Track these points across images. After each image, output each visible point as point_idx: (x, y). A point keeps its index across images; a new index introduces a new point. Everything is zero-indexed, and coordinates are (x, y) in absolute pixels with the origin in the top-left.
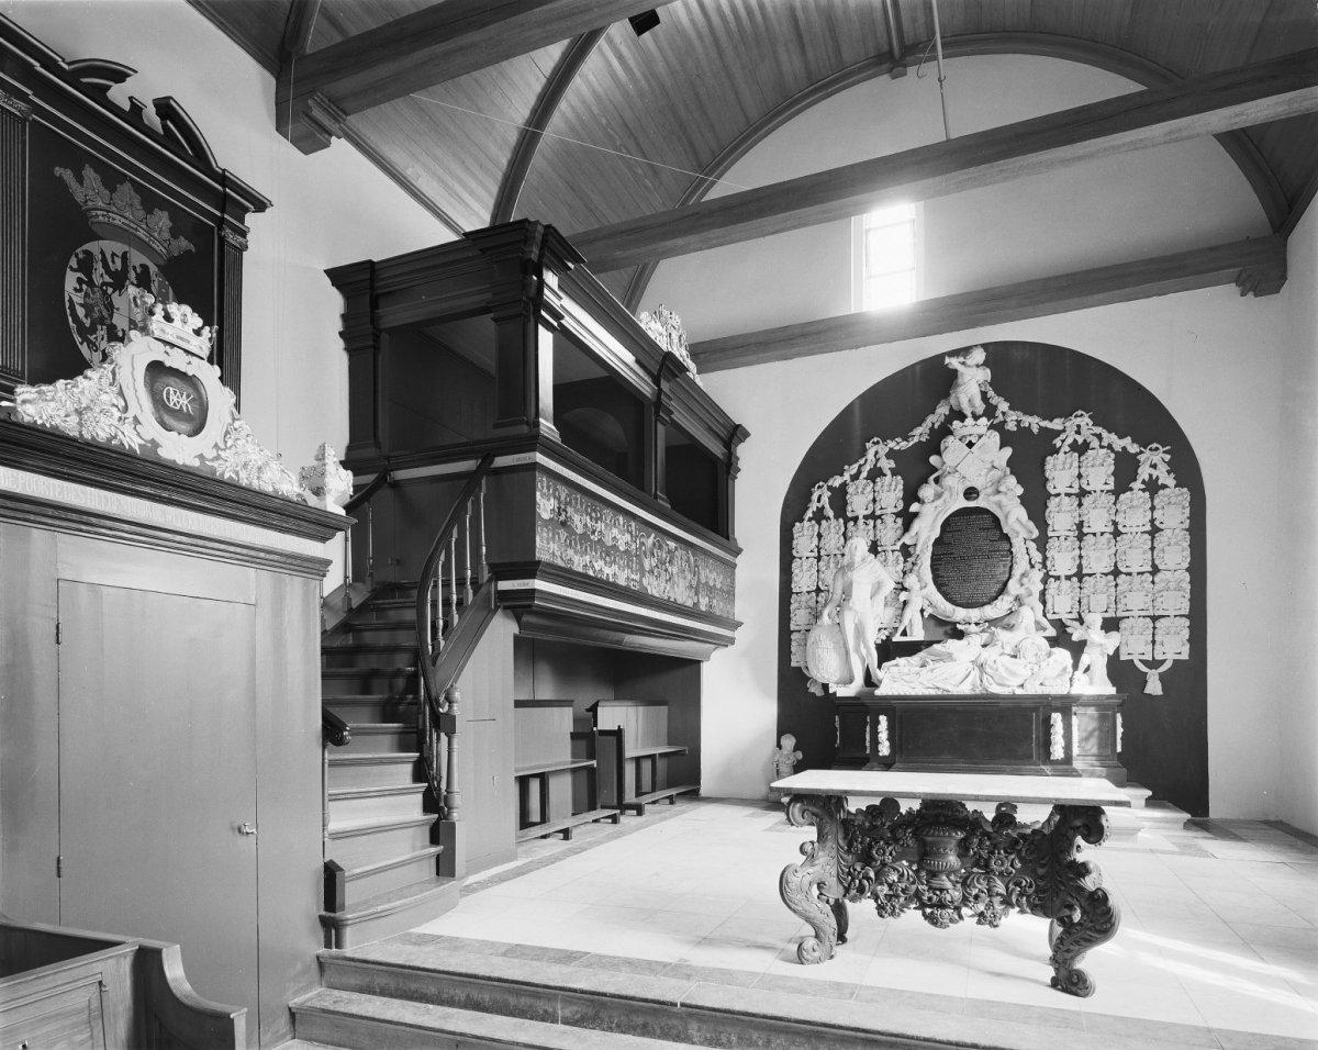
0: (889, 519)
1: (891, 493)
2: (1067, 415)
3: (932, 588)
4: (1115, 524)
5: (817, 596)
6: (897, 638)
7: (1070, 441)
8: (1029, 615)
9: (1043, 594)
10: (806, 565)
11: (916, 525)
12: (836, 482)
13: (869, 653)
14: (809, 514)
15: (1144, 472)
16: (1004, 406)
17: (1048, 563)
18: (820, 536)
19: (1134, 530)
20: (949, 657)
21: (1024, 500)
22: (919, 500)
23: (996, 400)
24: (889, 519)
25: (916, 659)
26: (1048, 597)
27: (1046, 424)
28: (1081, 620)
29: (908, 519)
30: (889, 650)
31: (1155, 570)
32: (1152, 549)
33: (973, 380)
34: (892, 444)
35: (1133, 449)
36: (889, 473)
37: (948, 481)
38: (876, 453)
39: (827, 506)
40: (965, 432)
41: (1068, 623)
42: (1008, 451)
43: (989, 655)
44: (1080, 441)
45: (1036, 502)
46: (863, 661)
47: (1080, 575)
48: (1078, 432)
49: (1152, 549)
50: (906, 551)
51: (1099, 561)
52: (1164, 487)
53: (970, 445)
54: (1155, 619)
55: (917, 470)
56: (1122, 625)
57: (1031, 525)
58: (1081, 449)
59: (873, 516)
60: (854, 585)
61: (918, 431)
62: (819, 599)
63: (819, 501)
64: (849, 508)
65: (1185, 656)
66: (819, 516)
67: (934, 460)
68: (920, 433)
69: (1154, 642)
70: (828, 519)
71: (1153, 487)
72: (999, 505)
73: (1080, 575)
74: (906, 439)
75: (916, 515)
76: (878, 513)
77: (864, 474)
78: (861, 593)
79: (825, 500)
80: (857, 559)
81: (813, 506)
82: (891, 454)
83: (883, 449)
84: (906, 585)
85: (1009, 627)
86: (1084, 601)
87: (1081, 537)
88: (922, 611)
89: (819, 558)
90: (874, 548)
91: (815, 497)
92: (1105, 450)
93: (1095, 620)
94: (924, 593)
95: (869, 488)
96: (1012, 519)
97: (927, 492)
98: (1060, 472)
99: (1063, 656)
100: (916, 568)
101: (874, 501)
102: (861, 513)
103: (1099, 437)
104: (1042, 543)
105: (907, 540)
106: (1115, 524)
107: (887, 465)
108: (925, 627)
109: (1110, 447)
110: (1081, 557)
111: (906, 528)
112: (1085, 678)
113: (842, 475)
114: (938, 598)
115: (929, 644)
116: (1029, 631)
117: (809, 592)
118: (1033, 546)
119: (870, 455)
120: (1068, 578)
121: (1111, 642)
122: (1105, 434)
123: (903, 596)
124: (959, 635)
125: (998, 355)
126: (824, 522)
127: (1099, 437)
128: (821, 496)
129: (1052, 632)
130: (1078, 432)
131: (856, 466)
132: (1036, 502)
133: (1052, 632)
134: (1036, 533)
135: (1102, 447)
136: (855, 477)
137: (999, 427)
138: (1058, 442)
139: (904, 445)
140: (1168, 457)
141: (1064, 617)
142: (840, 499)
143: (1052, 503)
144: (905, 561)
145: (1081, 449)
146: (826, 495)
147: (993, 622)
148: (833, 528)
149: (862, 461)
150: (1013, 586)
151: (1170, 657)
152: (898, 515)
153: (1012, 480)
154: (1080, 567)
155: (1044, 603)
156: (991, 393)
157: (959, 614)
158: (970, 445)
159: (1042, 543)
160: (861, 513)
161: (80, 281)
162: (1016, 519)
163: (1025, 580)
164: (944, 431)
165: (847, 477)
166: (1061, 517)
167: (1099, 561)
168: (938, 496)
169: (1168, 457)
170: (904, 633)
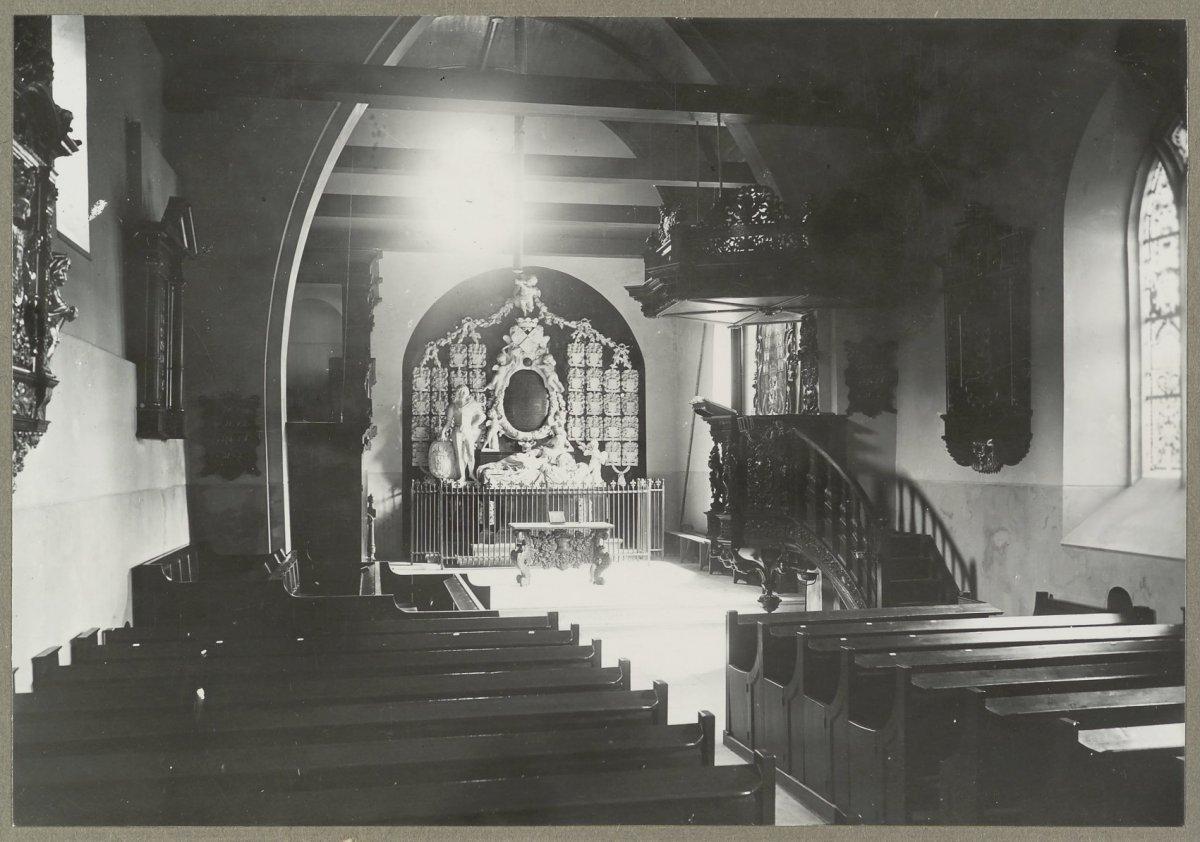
3: (504, 419)
5: (430, 418)
6: (484, 450)
7: (580, 336)
8: (562, 439)
9: (566, 425)
11: (497, 379)
12: (443, 344)
15: (617, 359)
16: (544, 309)
17: (569, 408)
19: (613, 391)
20: (520, 465)
26: (569, 427)
27: (567, 323)
29: (490, 376)
31: (622, 416)
34: (478, 323)
35: (612, 345)
37: (516, 353)
39: (436, 358)
40: (522, 325)
42: (548, 338)
45: (563, 371)
48: (584, 331)
50: (488, 394)
51: (595, 407)
52: (627, 368)
53: (527, 332)
54: (622, 443)
56: (608, 445)
57: (560, 384)
61: (495, 317)
62: (433, 421)
65: (636, 464)
67: (505, 338)
68: (496, 319)
69: (622, 456)
71: (621, 368)
72: (543, 370)
74: (487, 320)
75: (496, 372)
76: (470, 367)
77: (461, 340)
78: (466, 421)
79: (435, 353)
80: (464, 400)
81: (427, 358)
85: (552, 446)
86: (588, 431)
93: (595, 443)
94: (500, 423)
95: (465, 350)
96: (551, 382)
97: (503, 359)
98: (575, 357)
103: (595, 336)
104: (566, 396)
105: (490, 387)
107: (476, 336)
109: (600, 342)
111: (489, 380)
116: (561, 449)
117: (425, 416)
118: (561, 397)
119: (465, 329)
120: (579, 417)
122: (598, 334)
126: (434, 369)
127: (595, 336)
128: (432, 352)
129: (571, 449)
131: (455, 334)
132: (563, 371)
134: (563, 389)
135: (596, 342)
136: (455, 341)
137: (541, 323)
140: (628, 352)
141: (578, 440)
142: (445, 355)
143: (572, 371)
144: (487, 400)
150: (550, 420)
151: (629, 464)
152: (483, 369)
155: (566, 430)
156: (537, 300)
157: (522, 435)
158: (527, 332)
159: (566, 396)
162: (553, 380)
166: (576, 383)
167: (595, 407)
168: (509, 362)
169: (628, 352)
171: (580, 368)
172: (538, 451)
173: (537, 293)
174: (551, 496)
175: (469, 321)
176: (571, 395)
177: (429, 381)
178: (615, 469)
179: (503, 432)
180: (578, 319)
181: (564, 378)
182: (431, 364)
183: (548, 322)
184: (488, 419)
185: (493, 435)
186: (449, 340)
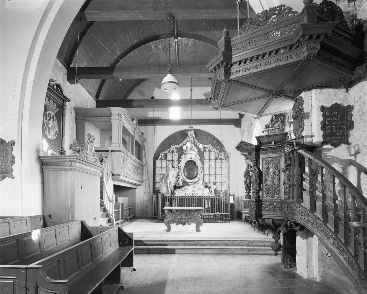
0: (176, 161)
1: (176, 156)
4: (215, 165)
6: (177, 185)
7: (208, 149)
9: (203, 177)
11: (181, 163)
12: (165, 152)
13: (172, 188)
14: (159, 159)
16: (197, 141)
18: (162, 163)
19: (219, 167)
20: (188, 189)
21: (200, 159)
22: (181, 158)
25: (181, 189)
28: (210, 183)
29: (179, 162)
30: (176, 187)
32: (221, 170)
34: (176, 146)
36: (175, 152)
38: (173, 147)
41: (207, 183)
43: (195, 189)
44: (210, 149)
45: (202, 160)
46: (171, 189)
47: (210, 174)
49: (221, 170)
51: (212, 172)
55: (181, 152)
56: (216, 184)
59: (172, 160)
60: (169, 174)
63: (161, 156)
64: (167, 158)
66: (161, 159)
69: (221, 187)
70: (163, 160)
71: (221, 159)
72: (196, 160)
73: (210, 174)
74: (179, 145)
76: (173, 160)
77: (171, 152)
79: (163, 156)
80: (170, 169)
81: (160, 157)
82: (176, 148)
83: (174, 147)
84: (179, 175)
87: (210, 167)
88: (182, 180)
89: (161, 168)
90: (173, 167)
91: (161, 155)
92: (214, 152)
93: (212, 183)
94: (182, 177)
96: (198, 163)
97: (183, 156)
98: (206, 155)
99: (207, 189)
100: (181, 171)
101: (173, 157)
102: (170, 159)
103: (213, 149)
104: (203, 168)
106: (215, 165)
107: (175, 150)
108: (182, 183)
109: (214, 151)
110: (210, 171)
111: (179, 163)
112: (211, 194)
113: (166, 151)
114: (185, 178)
116: (200, 185)
117: (159, 175)
118: (202, 168)
119: (172, 148)
120: (208, 175)
121: (215, 187)
122: (214, 149)
123: (178, 177)
124: (189, 185)
125: (196, 131)
127: (213, 149)
128: (162, 155)
130: (209, 148)
132: (202, 160)
133: (205, 185)
134: (202, 166)
136: (169, 152)
138: (206, 149)
141: (207, 182)
142: (166, 156)
143: (205, 160)
144: (179, 170)
146: (163, 155)
147: (195, 183)
148: (164, 163)
149: (170, 149)
152: (177, 160)
153: (198, 156)
154: (210, 173)
155: (204, 179)
156: (195, 139)
157: (188, 181)
160: (170, 159)
161: (46, 119)
162: (199, 163)
163: (200, 176)
165: (167, 152)
166: (206, 163)
167: (212, 172)
170: (178, 184)
171: (208, 159)
174: (195, 198)
175: (173, 146)
177: (161, 164)
178: (219, 191)
179: (183, 180)
180: (208, 144)
181: (203, 165)
182: (161, 159)
185: (180, 180)
186: (167, 152)
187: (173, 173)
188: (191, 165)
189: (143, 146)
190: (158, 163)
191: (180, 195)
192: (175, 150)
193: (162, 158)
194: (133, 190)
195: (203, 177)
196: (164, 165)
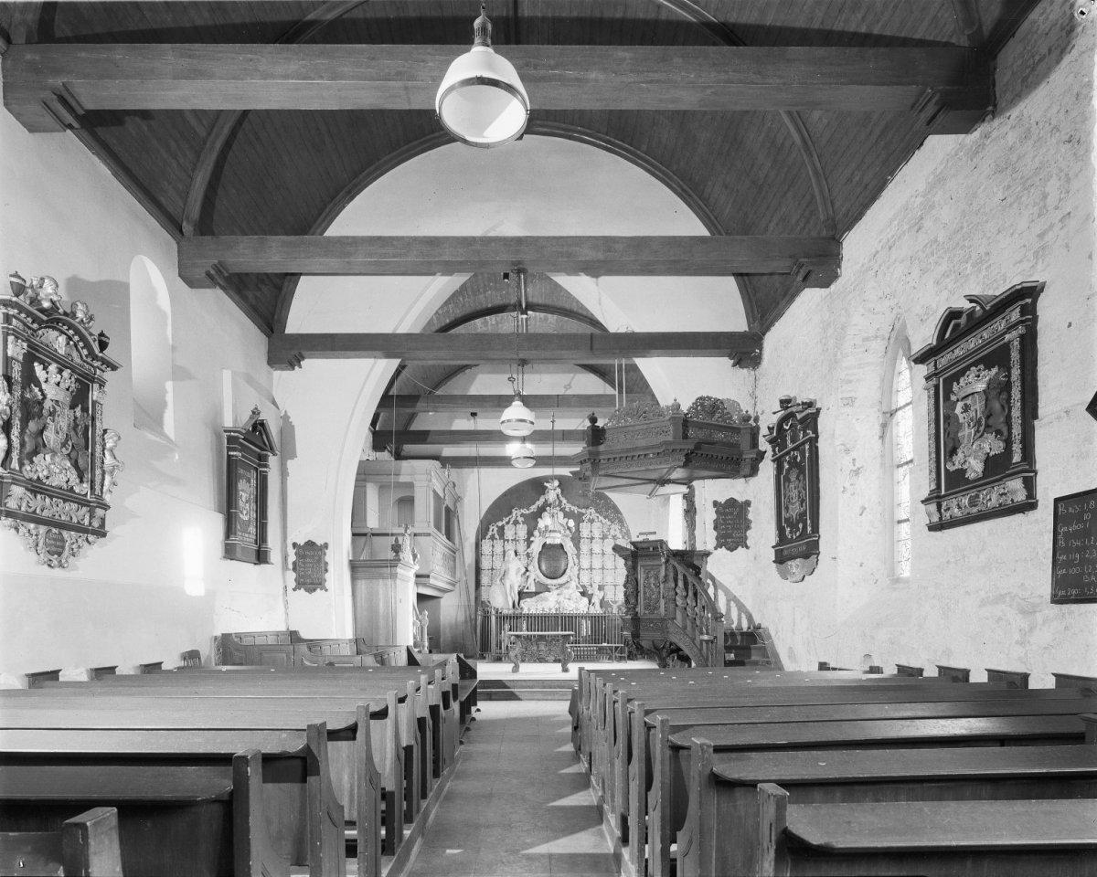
1: (522, 531)
2: (587, 508)
6: (525, 590)
8: (573, 584)
9: (579, 574)
10: (488, 557)
11: (533, 546)
12: (500, 524)
14: (488, 537)
16: (564, 501)
20: (546, 599)
23: (562, 499)
24: (522, 541)
25: (534, 599)
29: (529, 543)
33: (553, 493)
43: (561, 598)
45: (576, 540)
47: (591, 569)
51: (597, 564)
57: (574, 549)
58: (592, 521)
66: (493, 538)
68: (533, 508)
73: (591, 569)
79: (495, 532)
81: (490, 533)
82: (522, 515)
83: (519, 513)
87: (592, 554)
93: (596, 586)
94: (535, 573)
98: (585, 530)
99: (585, 600)
104: (578, 556)
107: (520, 519)
111: (529, 547)
115: (536, 593)
116: (572, 591)
119: (514, 515)
121: (601, 595)
123: (528, 573)
128: (493, 529)
132: (576, 540)
136: (508, 523)
139: (527, 512)
143: (582, 541)
145: (592, 521)
146: (496, 529)
147: (561, 585)
148: (499, 545)
157: (549, 581)
162: (569, 546)
163: (572, 571)
164: (542, 510)
165: (504, 522)
166: (584, 547)
167: (597, 564)
172: (558, 591)
173: (559, 491)
174: (562, 617)
176: (582, 556)
181: (578, 548)
182: (493, 538)
183: (567, 510)
184: (527, 570)
185: (531, 581)
186: (504, 522)
187: (515, 566)
188: (552, 553)
189: (455, 512)
190: (486, 546)
191: (533, 611)
192: (520, 519)
193: (493, 535)
194: (435, 601)
195: (579, 574)
196: (499, 549)
